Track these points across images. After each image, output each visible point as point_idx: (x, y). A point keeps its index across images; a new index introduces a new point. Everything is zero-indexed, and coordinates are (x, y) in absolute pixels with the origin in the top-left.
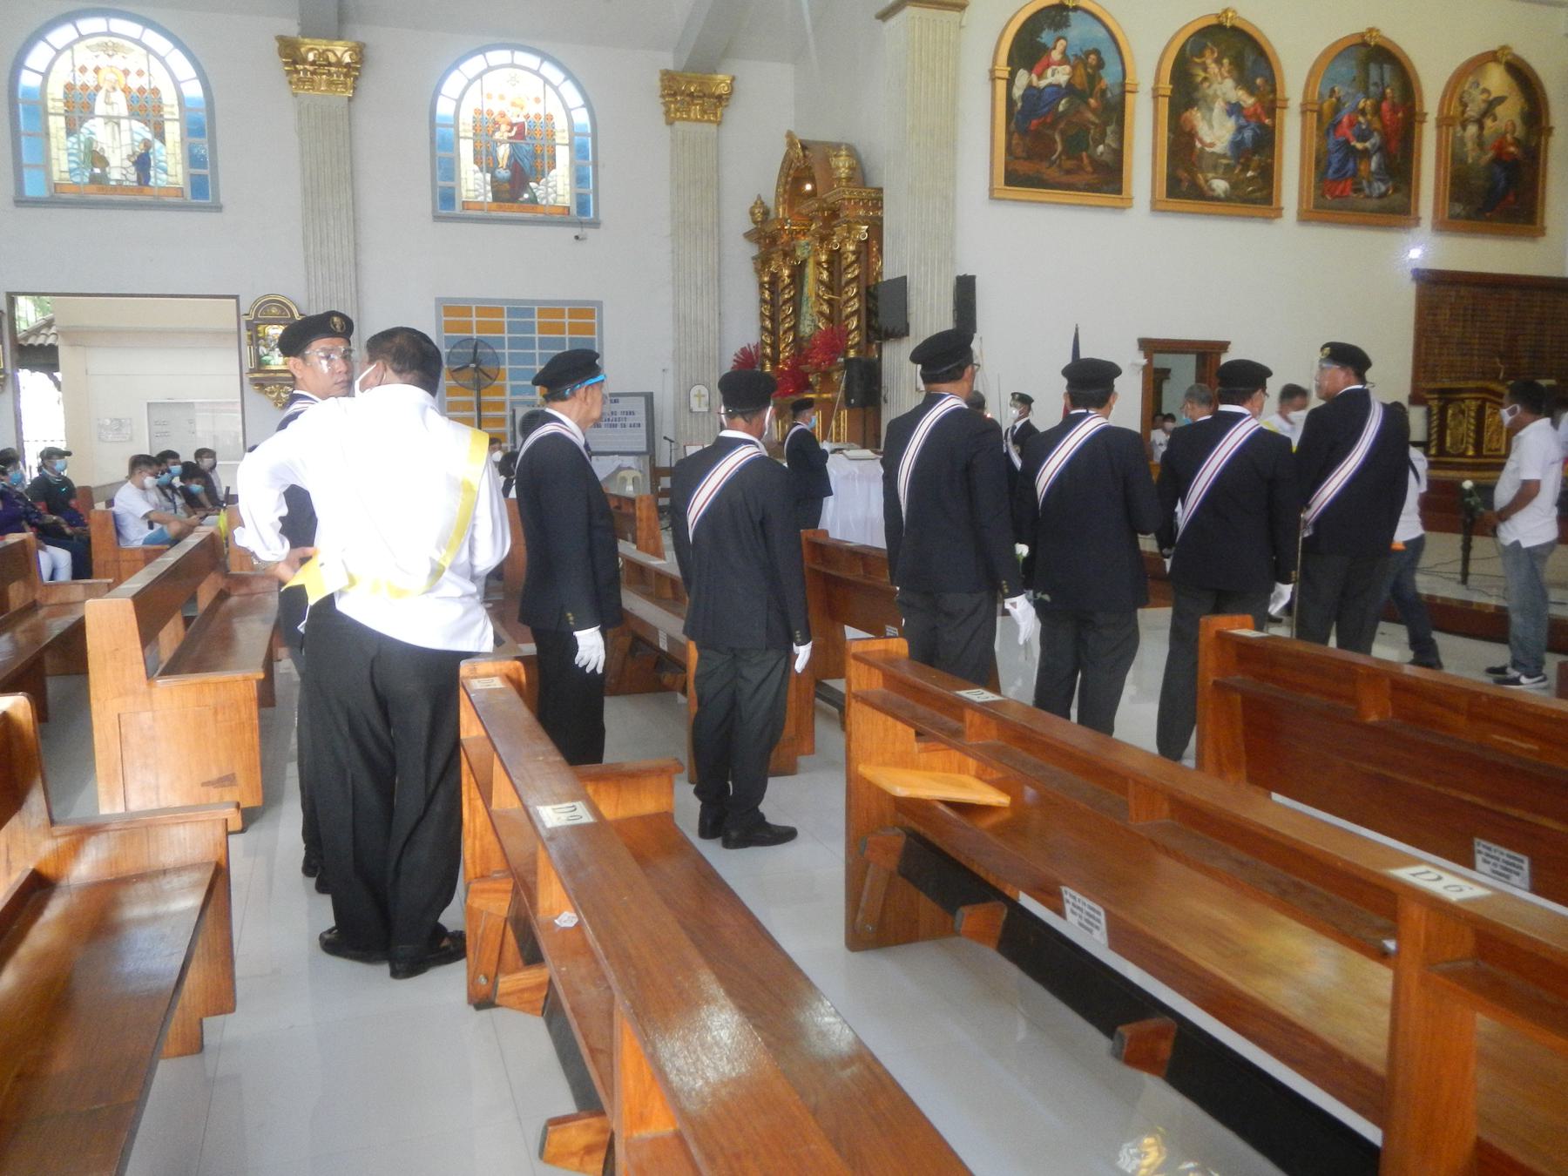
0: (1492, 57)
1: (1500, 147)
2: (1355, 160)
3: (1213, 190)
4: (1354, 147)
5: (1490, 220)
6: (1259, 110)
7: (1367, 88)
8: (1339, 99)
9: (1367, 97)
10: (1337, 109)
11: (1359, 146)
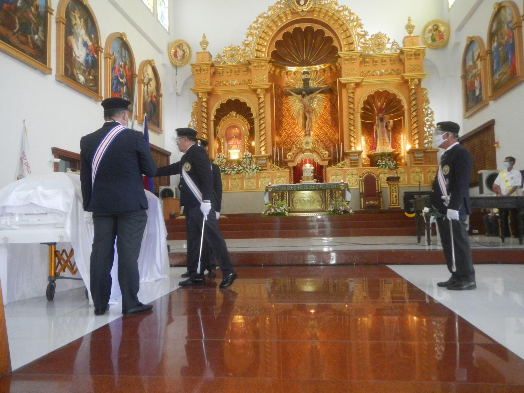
0: (149, 62)
1: (152, 97)
2: (120, 85)
3: (79, 79)
4: (119, 80)
5: (151, 123)
6: (93, 50)
7: (122, 58)
8: (115, 57)
9: (122, 62)
10: (114, 62)
11: (121, 80)
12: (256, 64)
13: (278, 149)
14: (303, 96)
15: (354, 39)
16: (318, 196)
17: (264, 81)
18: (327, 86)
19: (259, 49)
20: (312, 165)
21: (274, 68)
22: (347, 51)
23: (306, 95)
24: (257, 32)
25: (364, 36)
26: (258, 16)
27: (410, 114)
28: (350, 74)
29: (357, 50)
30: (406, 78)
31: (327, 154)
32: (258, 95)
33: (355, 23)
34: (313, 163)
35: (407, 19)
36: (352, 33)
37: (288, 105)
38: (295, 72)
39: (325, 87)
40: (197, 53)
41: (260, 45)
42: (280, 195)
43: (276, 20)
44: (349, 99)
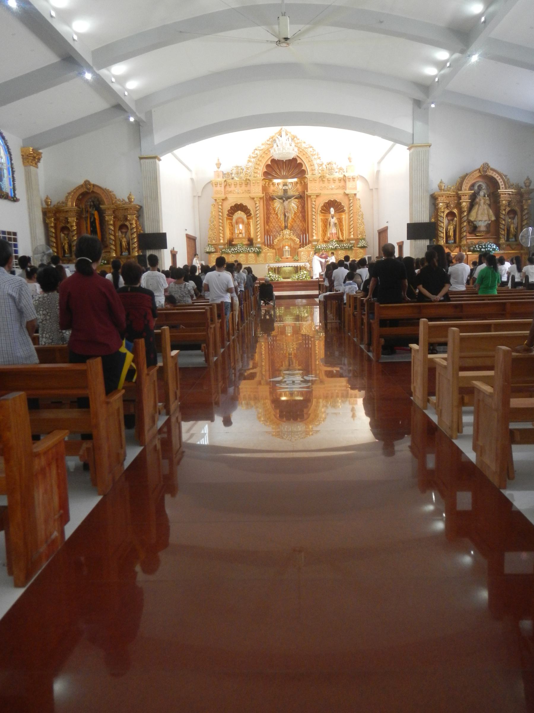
12: (254, 182)
14: (284, 201)
19: (256, 172)
24: (255, 160)
25: (321, 165)
26: (255, 149)
27: (349, 215)
31: (299, 241)
32: (255, 201)
34: (290, 246)
40: (214, 172)
41: (257, 169)
43: (266, 152)
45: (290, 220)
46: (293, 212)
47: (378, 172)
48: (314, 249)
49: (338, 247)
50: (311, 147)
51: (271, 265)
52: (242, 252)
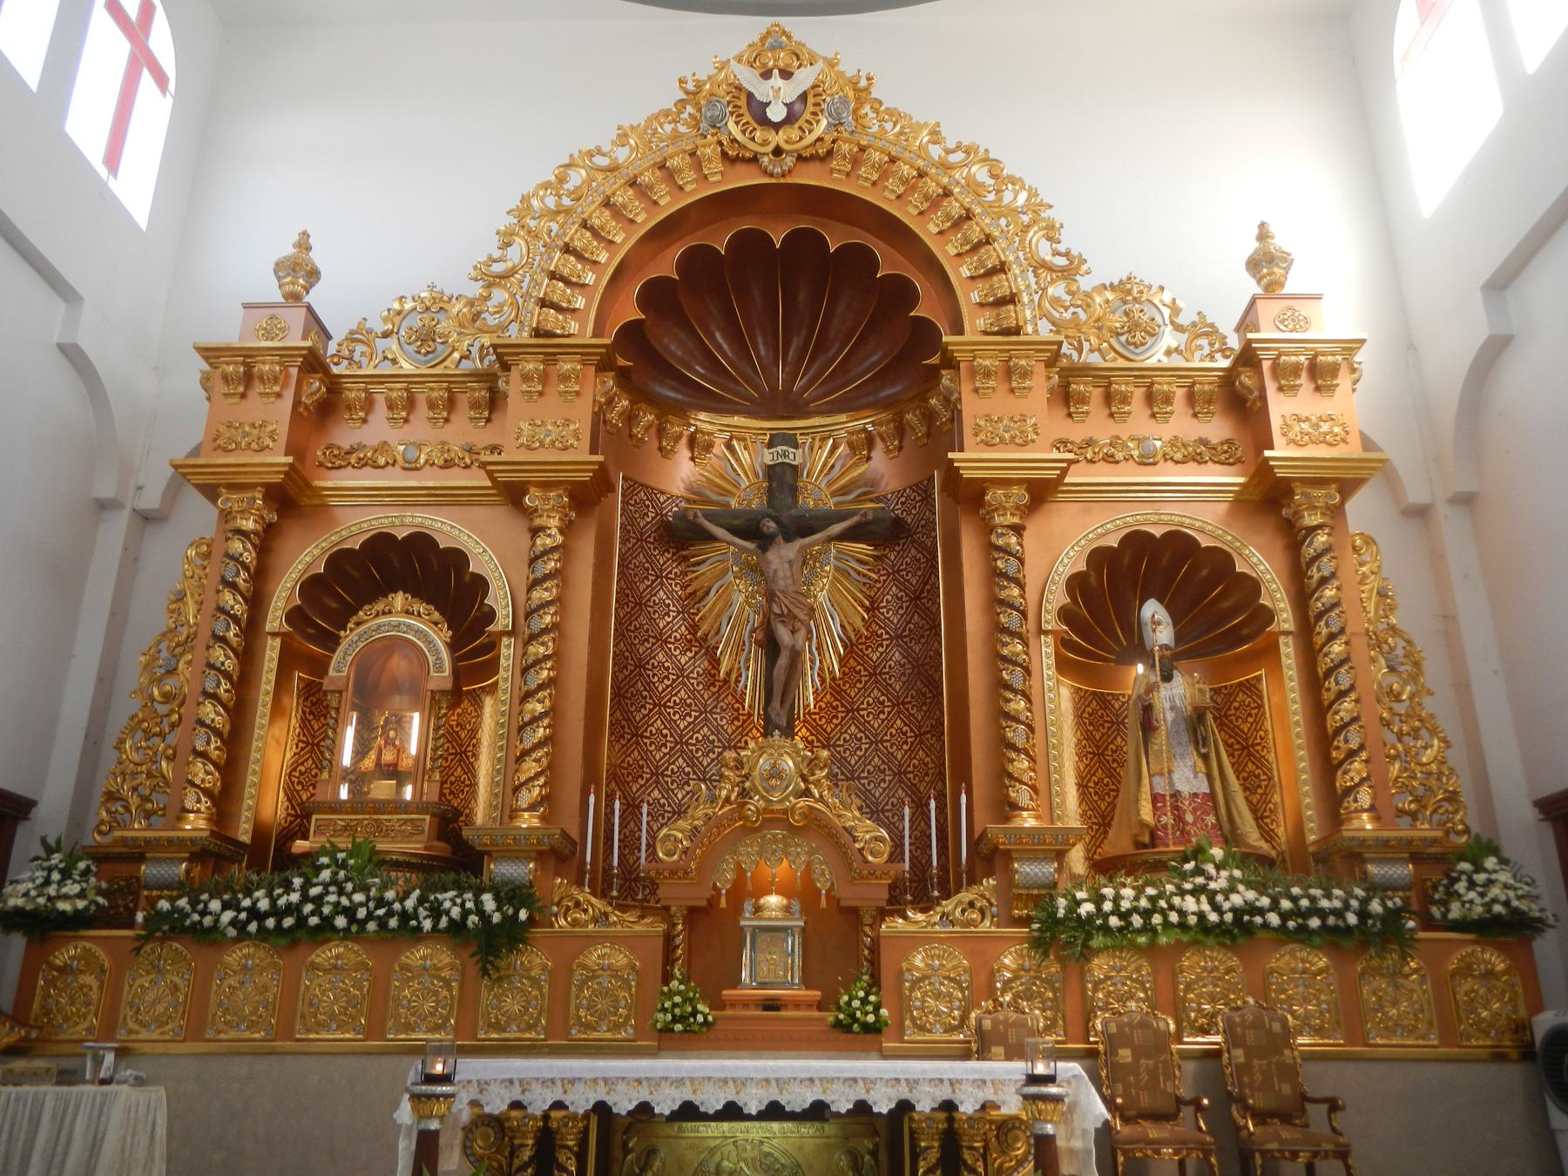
12: (531, 366)
13: (617, 805)
14: (764, 542)
15: (1022, 288)
16: (844, 1162)
17: (566, 449)
18: (881, 505)
20: (796, 906)
21: (626, 403)
22: (986, 333)
23: (780, 539)
24: (555, 227)
26: (567, 161)
27: (1310, 653)
28: (1002, 440)
29: (1036, 331)
30: (1280, 473)
31: (885, 849)
33: (1025, 219)
35: (1256, 231)
36: (1011, 258)
37: (689, 585)
38: (732, 438)
39: (873, 509)
40: (247, 306)
42: (526, 1154)
43: (646, 178)
44: (996, 560)
45: (808, 694)
46: (836, 629)
47: (1494, 351)
48: (1025, 921)
49: (1261, 912)
50: (986, 160)
51: (470, 1068)
52: (341, 922)
